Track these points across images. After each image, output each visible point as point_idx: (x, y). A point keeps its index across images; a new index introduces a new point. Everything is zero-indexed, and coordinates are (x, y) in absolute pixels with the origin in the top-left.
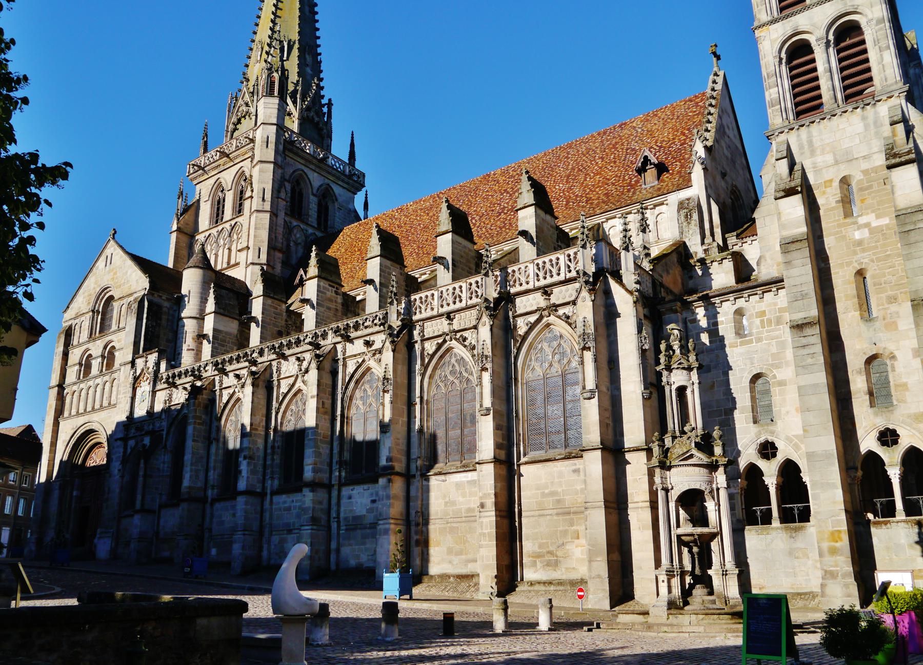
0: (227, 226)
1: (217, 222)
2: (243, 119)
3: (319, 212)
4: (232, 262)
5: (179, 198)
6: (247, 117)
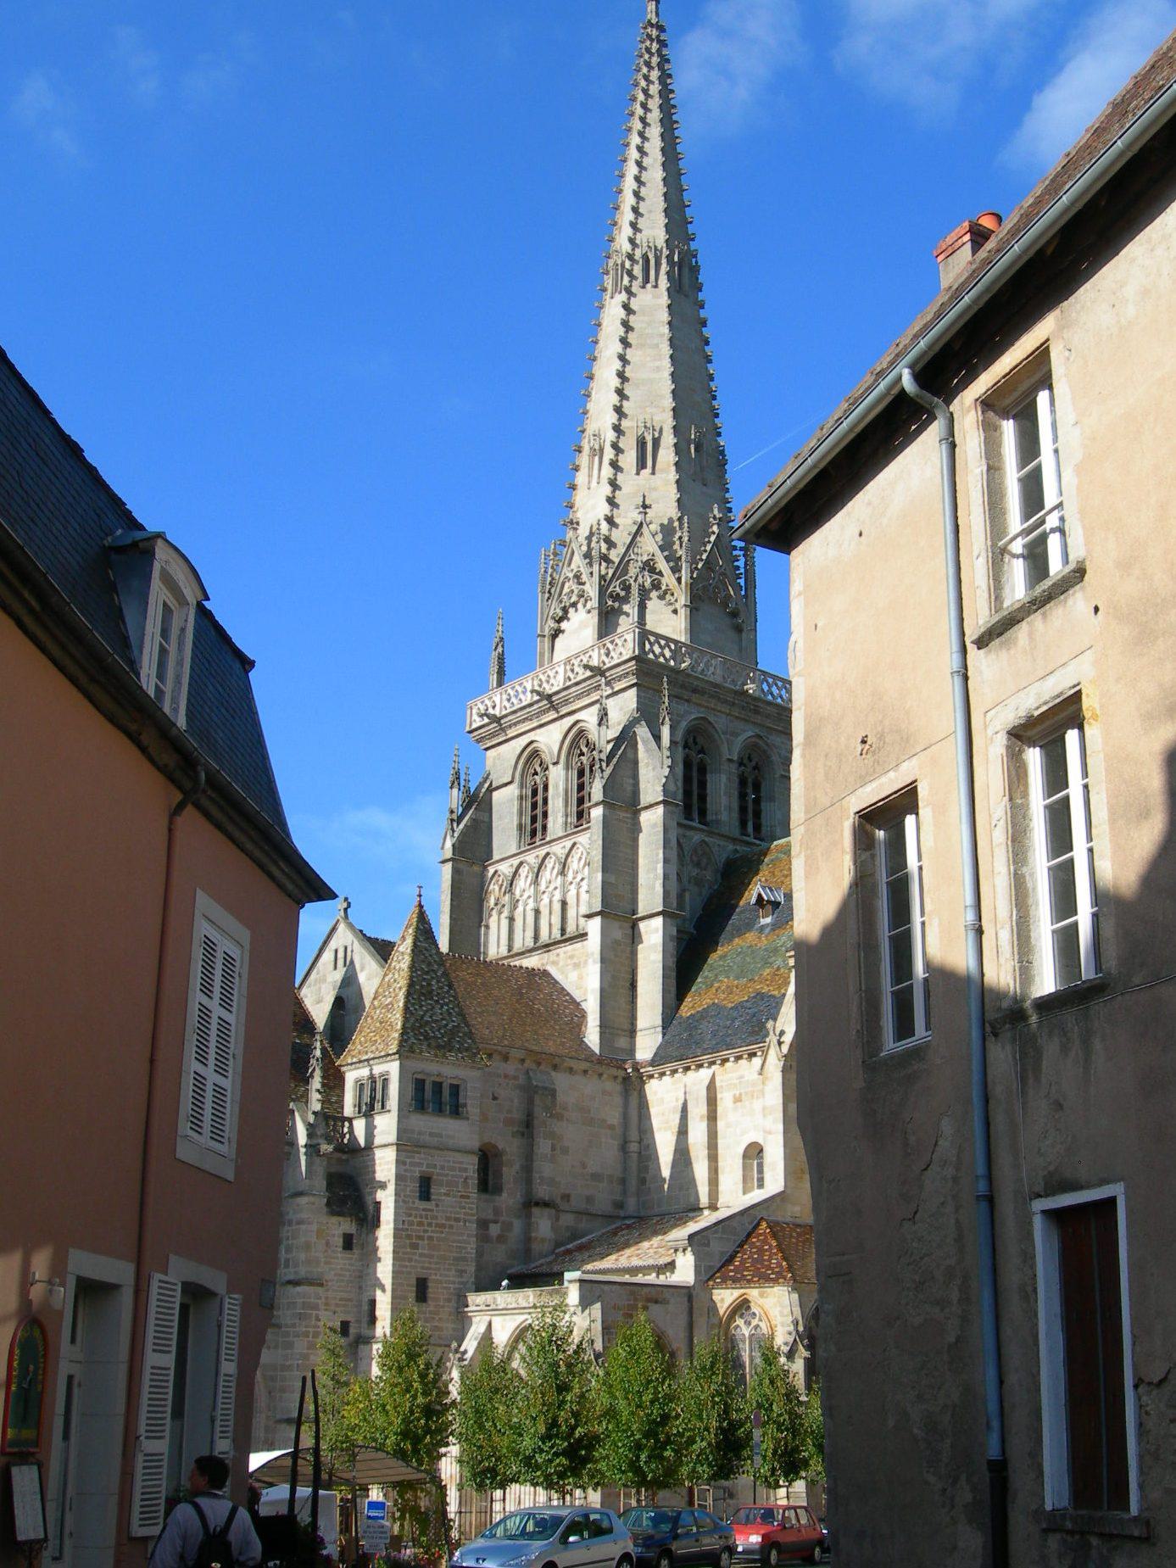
0: (559, 849)
1: (533, 833)
2: (571, 610)
3: (743, 796)
4: (571, 929)
5: (451, 788)
6: (580, 606)
